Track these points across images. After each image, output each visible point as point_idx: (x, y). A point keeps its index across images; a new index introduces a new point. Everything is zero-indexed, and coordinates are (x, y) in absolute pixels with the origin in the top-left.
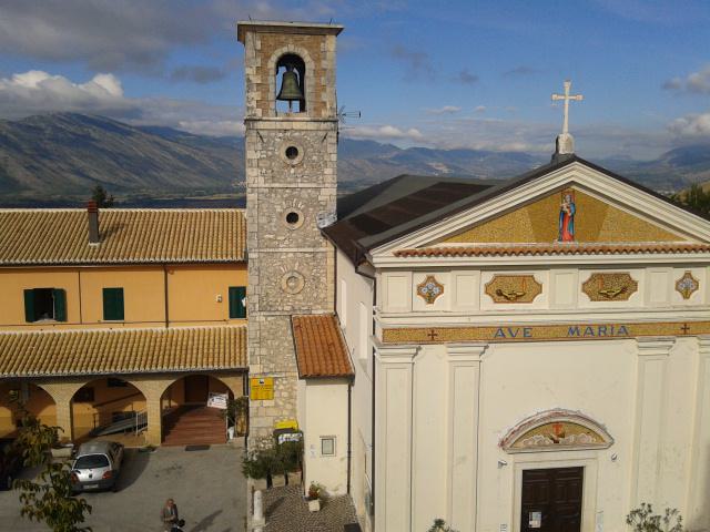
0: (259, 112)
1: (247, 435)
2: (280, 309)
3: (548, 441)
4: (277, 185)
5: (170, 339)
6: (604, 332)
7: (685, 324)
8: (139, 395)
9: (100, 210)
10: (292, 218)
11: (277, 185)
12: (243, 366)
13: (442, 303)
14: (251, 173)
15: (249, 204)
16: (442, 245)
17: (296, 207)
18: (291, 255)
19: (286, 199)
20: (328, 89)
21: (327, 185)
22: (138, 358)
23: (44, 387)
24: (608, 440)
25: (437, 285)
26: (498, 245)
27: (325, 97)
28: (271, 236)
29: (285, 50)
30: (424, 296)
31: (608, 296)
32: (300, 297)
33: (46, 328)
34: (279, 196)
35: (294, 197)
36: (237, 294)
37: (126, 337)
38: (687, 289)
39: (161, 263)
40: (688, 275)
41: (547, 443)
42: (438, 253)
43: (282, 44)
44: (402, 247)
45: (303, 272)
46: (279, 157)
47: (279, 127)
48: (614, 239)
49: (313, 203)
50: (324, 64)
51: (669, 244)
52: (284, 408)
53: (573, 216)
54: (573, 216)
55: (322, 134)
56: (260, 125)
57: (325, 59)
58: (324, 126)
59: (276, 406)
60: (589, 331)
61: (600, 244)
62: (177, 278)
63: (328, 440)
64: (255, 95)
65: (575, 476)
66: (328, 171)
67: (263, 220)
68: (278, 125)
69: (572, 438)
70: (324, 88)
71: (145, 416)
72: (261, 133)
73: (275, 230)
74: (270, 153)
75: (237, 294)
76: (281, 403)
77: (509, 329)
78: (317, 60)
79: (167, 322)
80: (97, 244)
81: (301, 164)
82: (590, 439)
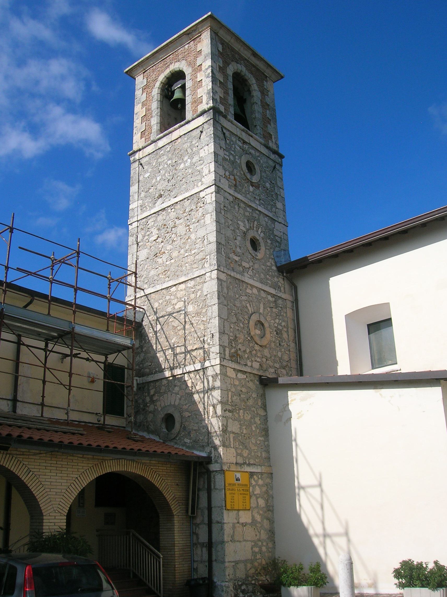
2: (249, 364)
4: (239, 196)
28: (237, 258)
32: (266, 352)
46: (240, 166)
47: (239, 134)
59: (254, 523)
76: (258, 518)
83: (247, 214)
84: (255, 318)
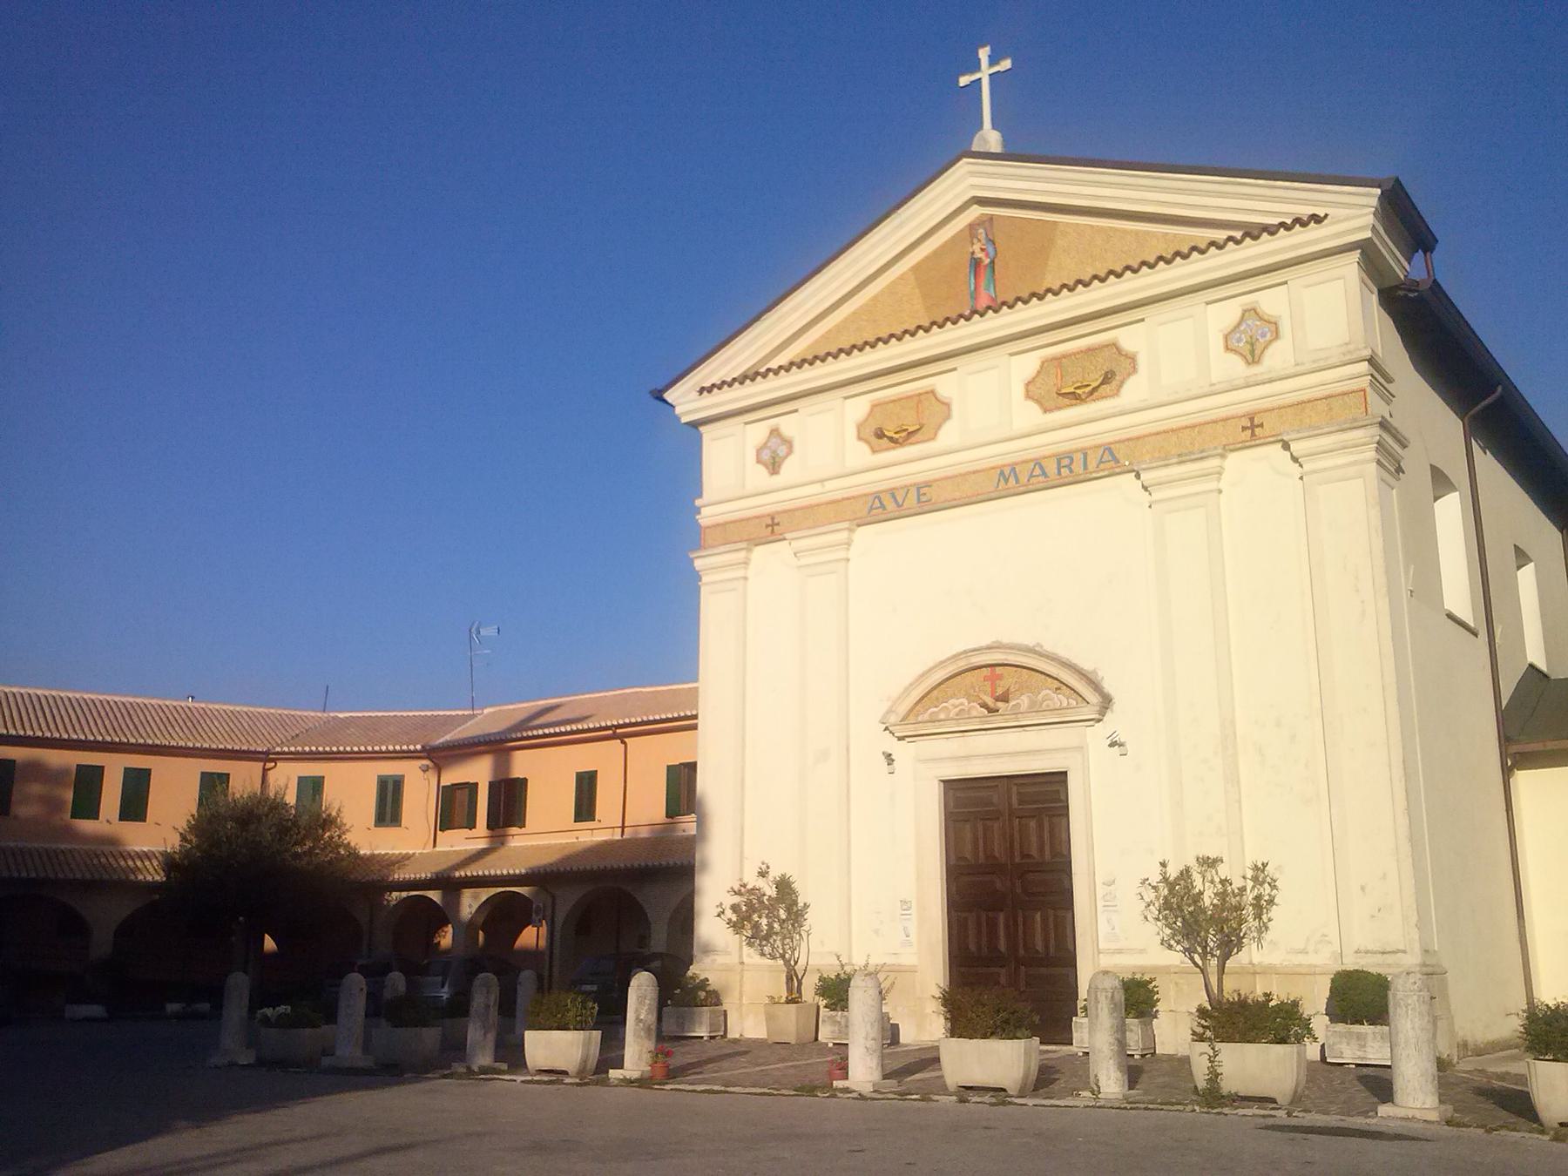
6: (1068, 466)
30: (766, 466)
41: (974, 713)
53: (992, 262)
54: (992, 262)
69: (1024, 701)
77: (892, 492)
82: (1061, 699)
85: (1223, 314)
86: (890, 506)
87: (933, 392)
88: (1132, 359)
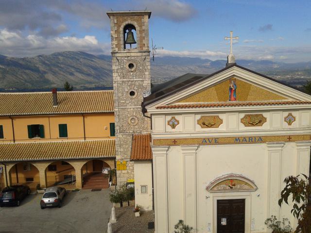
0: (117, 49)
1: (116, 185)
2: (128, 132)
3: (228, 188)
4: (125, 80)
5: (86, 145)
7: (289, 136)
8: (72, 169)
9: (58, 92)
10: (132, 93)
11: (125, 80)
12: (114, 156)
13: (179, 128)
14: (115, 75)
15: (114, 88)
16: (177, 104)
17: (134, 89)
18: (132, 109)
19: (129, 86)
20: (146, 39)
21: (146, 79)
22: (72, 153)
23: (34, 165)
24: (255, 188)
25: (176, 121)
26: (202, 103)
27: (144, 42)
29: (127, 23)
30: (171, 125)
31: (253, 125)
32: (136, 127)
33: (37, 141)
34: (126, 84)
35: (132, 84)
36: (112, 126)
37: (68, 144)
38: (290, 121)
39: (81, 113)
40: (290, 114)
41: (227, 188)
42: (175, 107)
43: (125, 20)
44: (159, 105)
45: (138, 116)
46: (125, 68)
48: (255, 99)
49: (141, 87)
50: (144, 28)
51: (280, 101)
52: (131, 173)
55: (144, 57)
56: (117, 55)
57: (144, 26)
58: (144, 54)
59: (128, 173)
60: (244, 140)
61: (248, 102)
62: (88, 120)
63: (144, 187)
64: (115, 42)
65: (242, 202)
66: (147, 73)
67: (120, 95)
68: (125, 55)
69: (239, 186)
70: (144, 38)
71: (75, 177)
72: (118, 58)
73: (125, 98)
74: (122, 66)
75: (112, 126)
76: (130, 172)
77: (208, 139)
78: (141, 26)
79: (85, 138)
80: (56, 106)
81: (135, 70)
82: (246, 187)
83: (129, 84)
84: (130, 118)
85: (286, 114)
86: (208, 142)
87: (218, 117)
88: (266, 119)
